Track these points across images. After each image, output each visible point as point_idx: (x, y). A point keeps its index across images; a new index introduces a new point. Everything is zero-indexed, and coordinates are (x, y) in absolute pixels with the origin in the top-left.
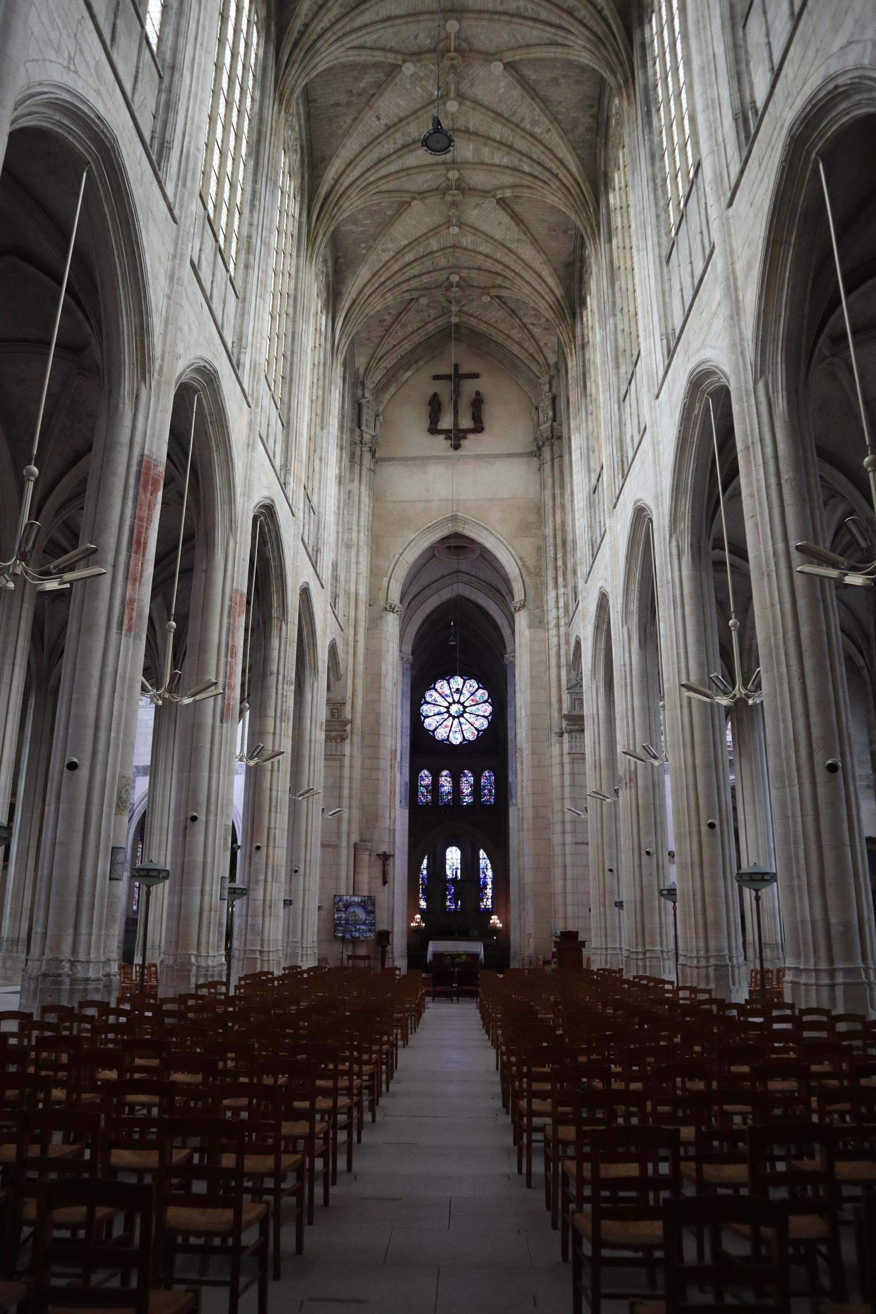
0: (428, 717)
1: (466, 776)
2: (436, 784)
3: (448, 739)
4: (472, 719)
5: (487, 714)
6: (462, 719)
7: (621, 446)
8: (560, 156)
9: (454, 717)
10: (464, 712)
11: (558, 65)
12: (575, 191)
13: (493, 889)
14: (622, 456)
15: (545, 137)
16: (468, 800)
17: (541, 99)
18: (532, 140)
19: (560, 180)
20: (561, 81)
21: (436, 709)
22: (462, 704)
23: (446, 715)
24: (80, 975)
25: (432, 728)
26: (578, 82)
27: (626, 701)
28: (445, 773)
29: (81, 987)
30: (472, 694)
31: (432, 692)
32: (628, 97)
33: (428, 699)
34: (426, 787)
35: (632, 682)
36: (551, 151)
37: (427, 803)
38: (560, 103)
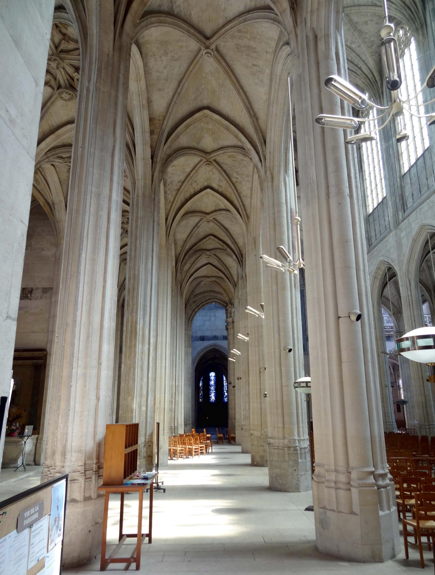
7: (403, 197)
8: (364, 59)
11: (369, 15)
12: (370, 76)
14: (403, 202)
15: (357, 50)
17: (358, 31)
18: (351, 51)
19: (362, 70)
20: (369, 22)
24: (302, 446)
26: (377, 23)
27: (411, 312)
29: (304, 451)
32: (423, 34)
35: (412, 304)
36: (359, 56)
38: (366, 33)
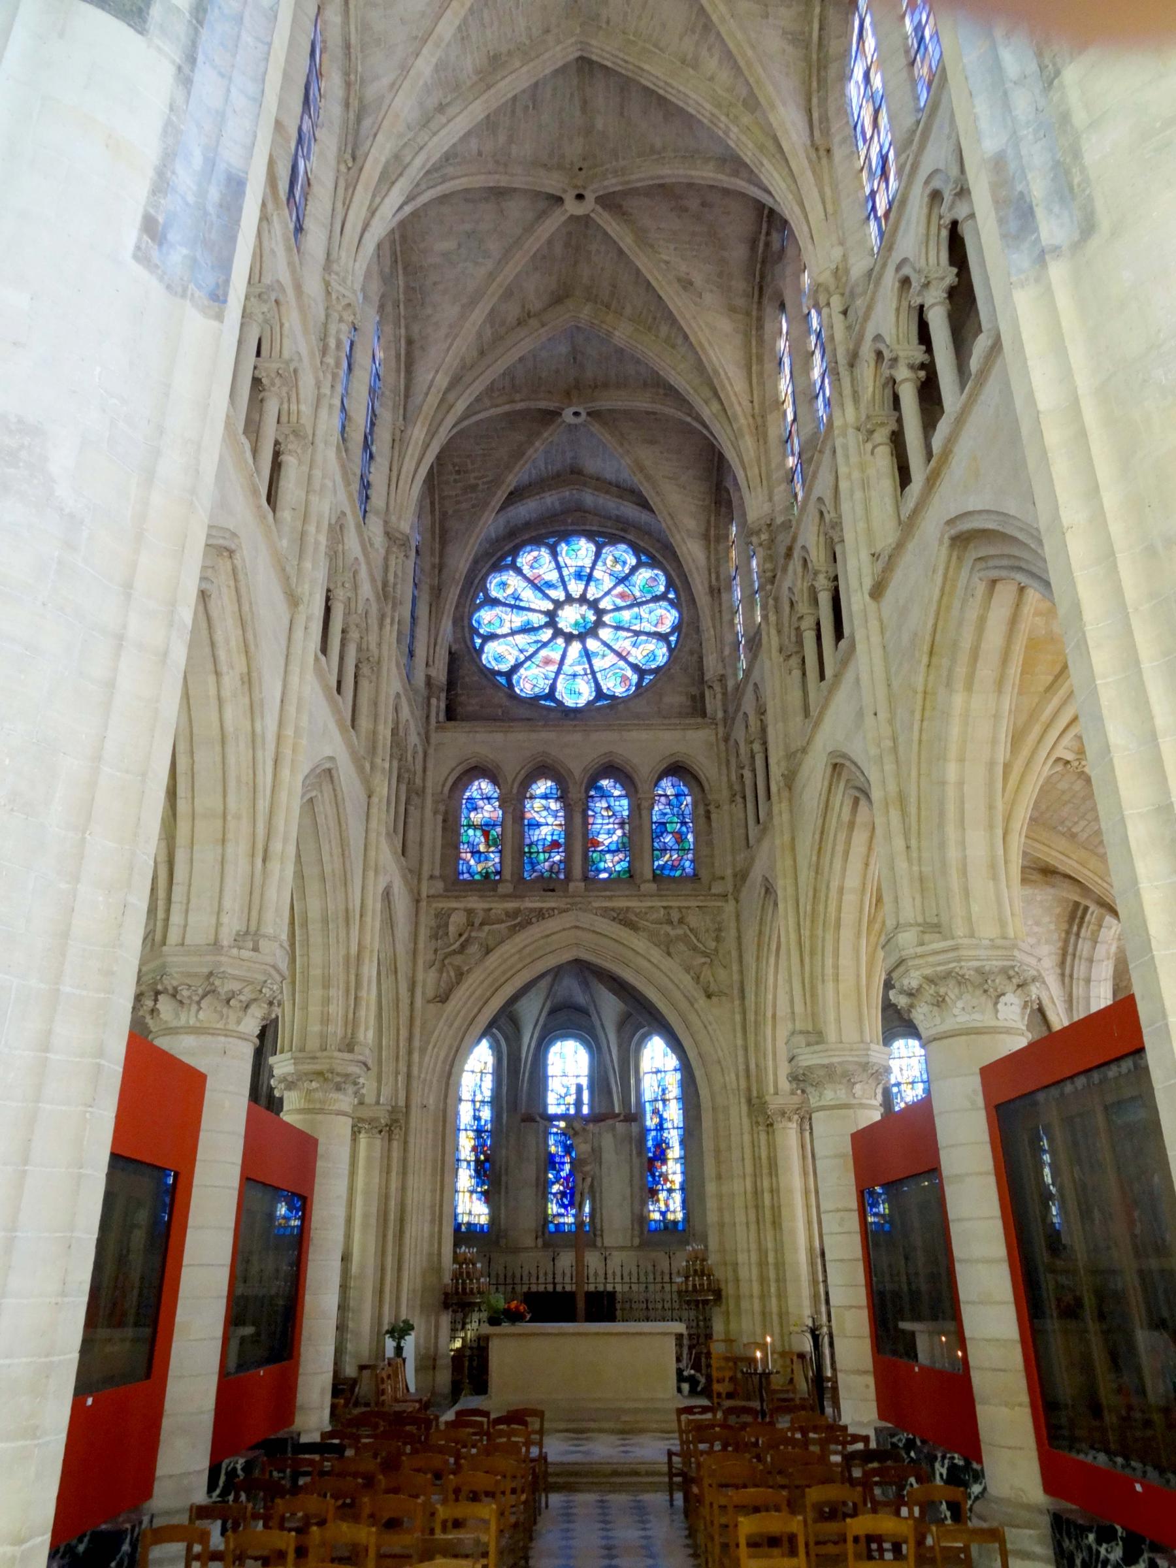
0: (493, 637)
1: (605, 795)
2: (516, 817)
3: (551, 695)
4: (623, 642)
5: (665, 628)
6: (592, 644)
9: (569, 638)
10: (599, 623)
13: (685, 1160)
16: (613, 864)
21: (518, 620)
22: (593, 605)
23: (547, 634)
25: (504, 667)
28: (542, 786)
30: (622, 580)
31: (511, 578)
33: (494, 593)
34: (485, 829)
37: (487, 876)
